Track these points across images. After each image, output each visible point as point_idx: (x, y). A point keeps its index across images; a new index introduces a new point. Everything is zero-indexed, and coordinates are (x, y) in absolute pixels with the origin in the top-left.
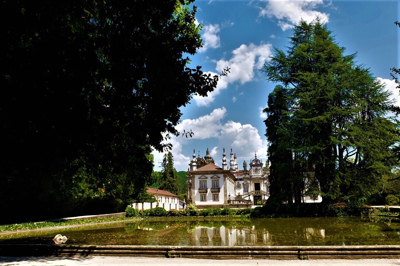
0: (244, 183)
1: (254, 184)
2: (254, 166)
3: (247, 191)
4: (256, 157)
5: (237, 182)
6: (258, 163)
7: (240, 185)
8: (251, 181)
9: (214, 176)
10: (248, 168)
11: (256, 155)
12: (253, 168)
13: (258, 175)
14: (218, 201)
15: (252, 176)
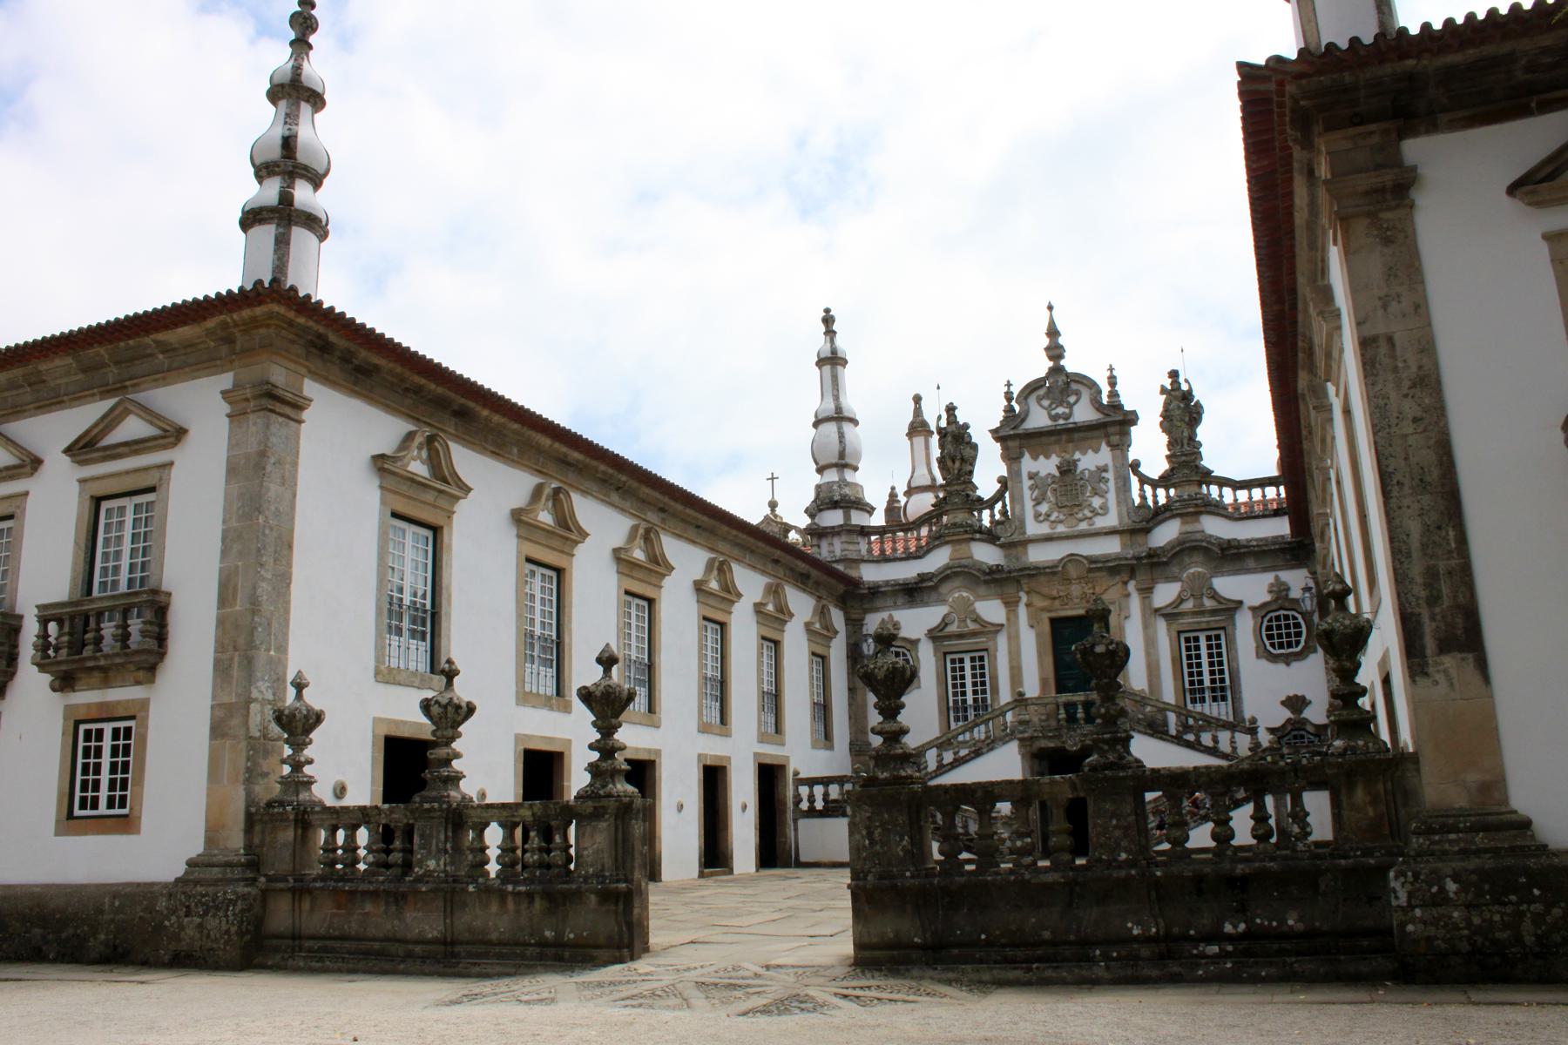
0: (945, 623)
1: (1046, 627)
2: (1035, 441)
3: (981, 705)
4: (1055, 351)
5: (873, 622)
6: (1084, 413)
7: (915, 643)
8: (1011, 605)
9: (109, 421)
10: (988, 473)
11: (1053, 332)
12: (1028, 464)
13: (1083, 526)
14: (126, 824)
15: (1025, 543)
